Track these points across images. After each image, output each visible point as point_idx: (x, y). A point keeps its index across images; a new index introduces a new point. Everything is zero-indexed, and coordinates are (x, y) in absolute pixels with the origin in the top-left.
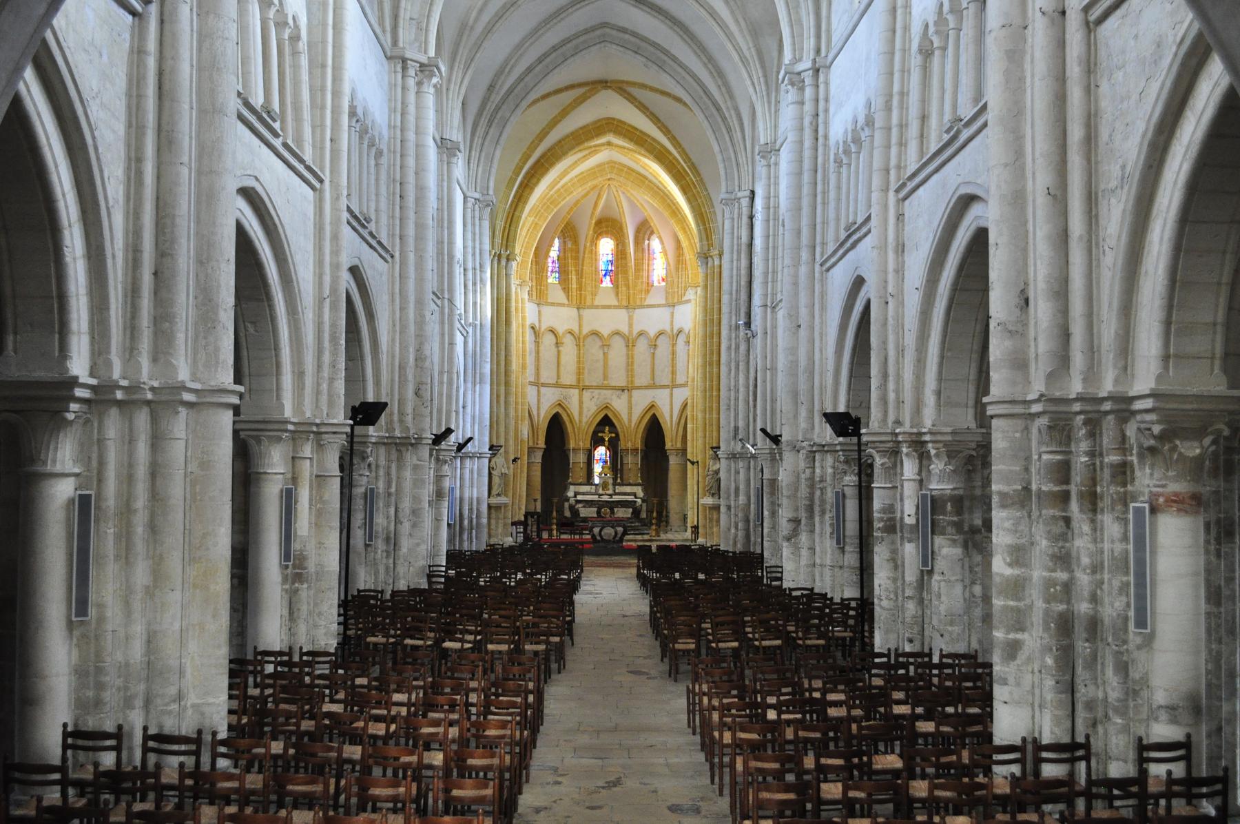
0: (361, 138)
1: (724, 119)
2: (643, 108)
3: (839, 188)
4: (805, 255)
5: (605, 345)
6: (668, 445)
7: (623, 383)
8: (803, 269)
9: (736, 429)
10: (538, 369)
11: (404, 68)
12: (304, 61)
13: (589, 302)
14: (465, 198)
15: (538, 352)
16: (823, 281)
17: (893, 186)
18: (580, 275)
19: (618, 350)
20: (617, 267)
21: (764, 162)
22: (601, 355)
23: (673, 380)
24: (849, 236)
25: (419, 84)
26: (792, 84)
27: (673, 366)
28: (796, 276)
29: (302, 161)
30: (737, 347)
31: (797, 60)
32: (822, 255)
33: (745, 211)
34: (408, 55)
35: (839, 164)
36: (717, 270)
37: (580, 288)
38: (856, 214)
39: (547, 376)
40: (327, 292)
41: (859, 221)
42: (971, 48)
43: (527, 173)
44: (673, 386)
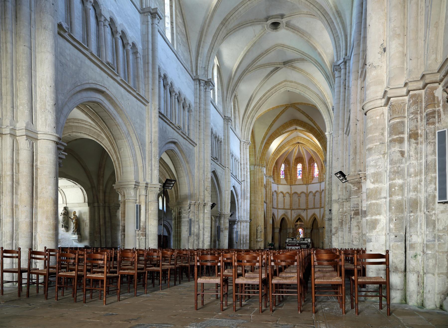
2: (303, 113)
5: (299, 196)
7: (305, 207)
11: (200, 83)
13: (294, 183)
18: (291, 175)
22: (298, 200)
23: (321, 206)
34: (200, 78)
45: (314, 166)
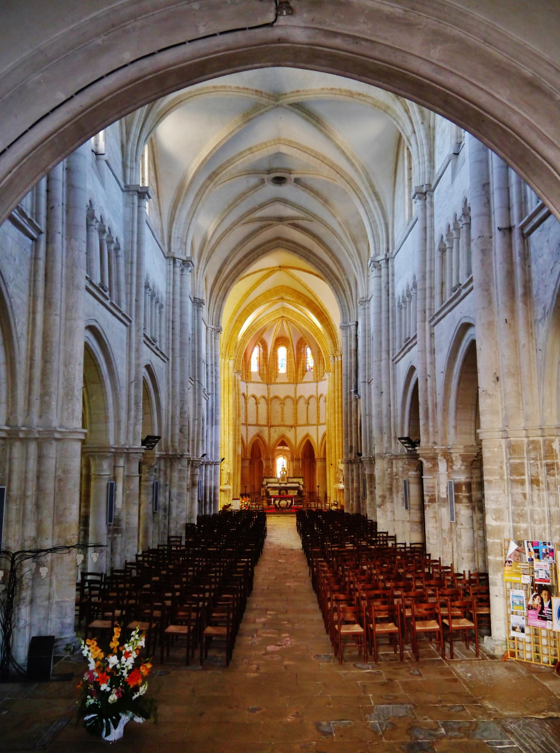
0: (152, 299)
1: (341, 285)
3: (400, 320)
4: (384, 355)
6: (316, 456)
7: (291, 423)
8: (383, 363)
9: (351, 447)
10: (246, 417)
11: (174, 262)
12: (122, 261)
13: (273, 381)
14: (207, 328)
15: (246, 408)
16: (394, 369)
17: (428, 319)
19: (289, 407)
20: (287, 362)
21: (362, 307)
22: (280, 410)
23: (318, 421)
24: (407, 345)
25: (182, 270)
26: (375, 267)
27: (318, 414)
28: (380, 366)
29: (120, 312)
30: (351, 402)
31: (377, 255)
32: (393, 355)
33: (353, 333)
34: (176, 256)
35: (400, 307)
36: (340, 363)
37: (268, 374)
38: (410, 333)
39: (252, 420)
40: (133, 379)
41: (412, 337)
42: (465, 248)
43: (240, 315)
44: (318, 424)
45: (305, 354)
